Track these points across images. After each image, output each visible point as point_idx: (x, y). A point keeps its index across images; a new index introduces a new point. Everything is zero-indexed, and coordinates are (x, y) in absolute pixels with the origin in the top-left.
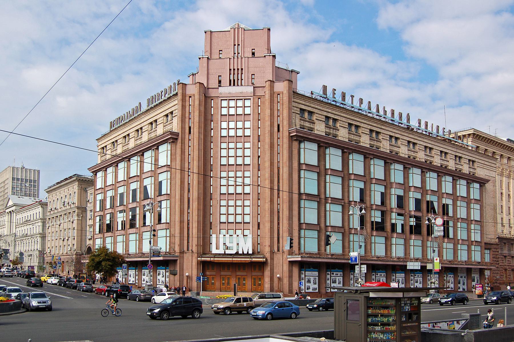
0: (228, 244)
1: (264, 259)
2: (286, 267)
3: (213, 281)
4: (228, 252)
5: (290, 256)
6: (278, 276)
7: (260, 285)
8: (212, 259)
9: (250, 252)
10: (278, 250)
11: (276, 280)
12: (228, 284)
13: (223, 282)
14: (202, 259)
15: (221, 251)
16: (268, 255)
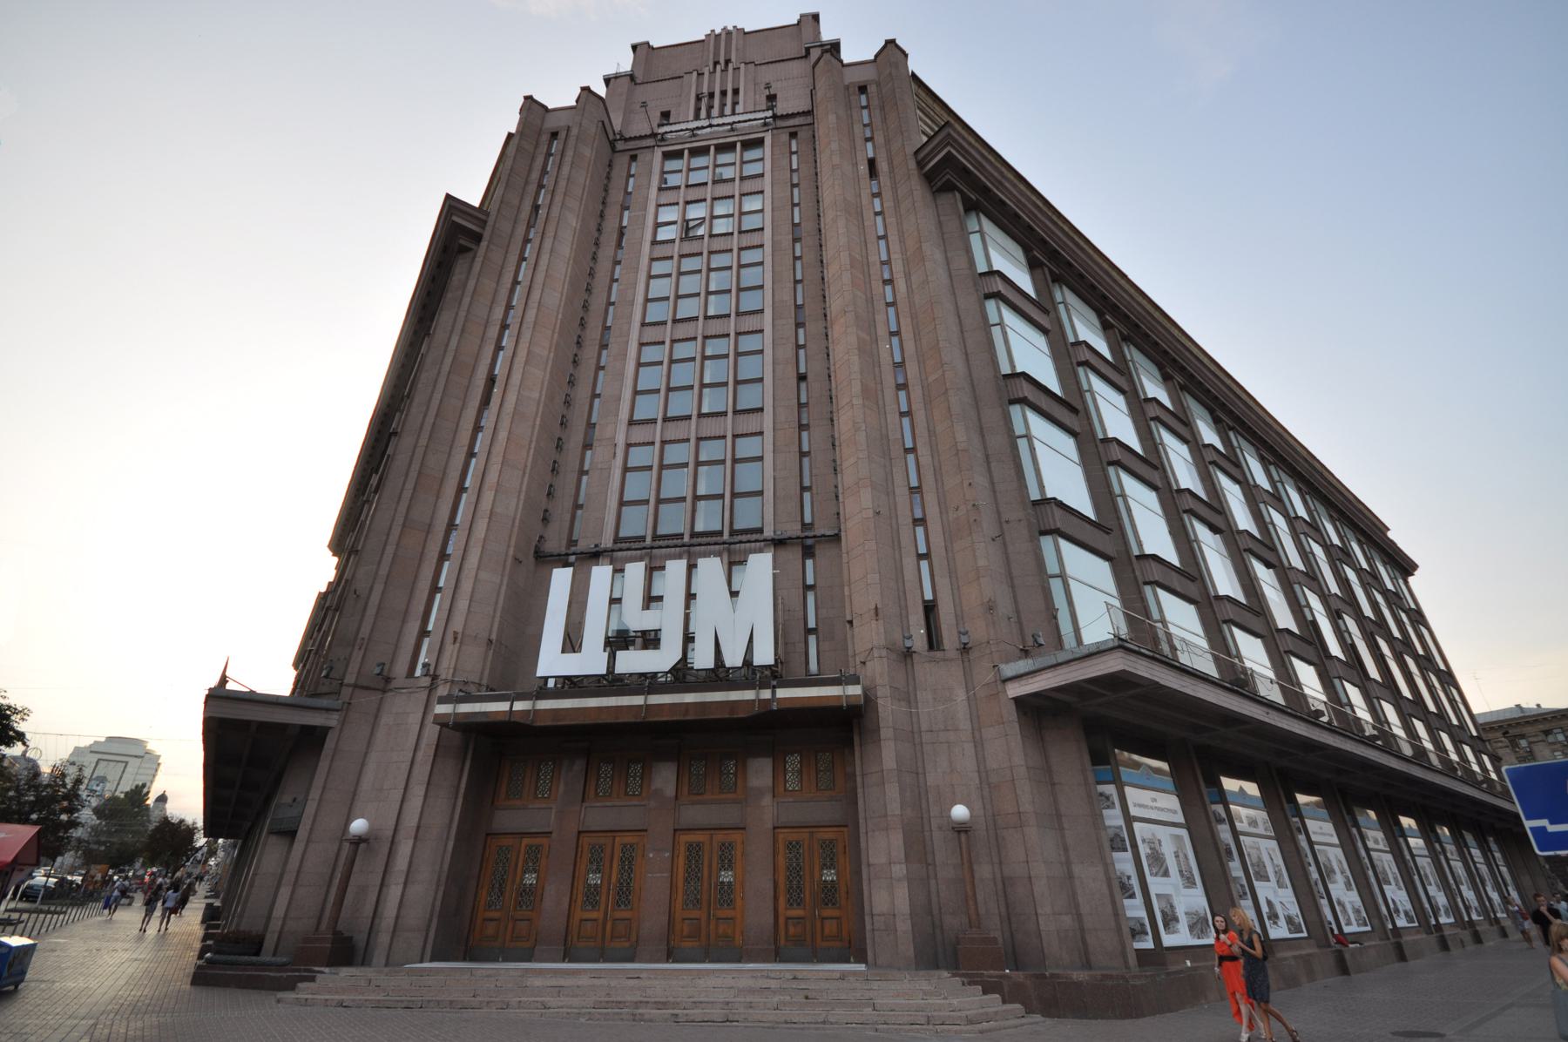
0: (636, 618)
1: (855, 690)
2: (1008, 746)
3: (530, 879)
4: (632, 662)
5: (1023, 665)
6: (960, 812)
7: (829, 894)
8: (519, 706)
9: (764, 655)
10: (933, 641)
11: (944, 853)
12: (624, 894)
13: (594, 879)
14: (465, 708)
15: (590, 660)
16: (879, 671)
